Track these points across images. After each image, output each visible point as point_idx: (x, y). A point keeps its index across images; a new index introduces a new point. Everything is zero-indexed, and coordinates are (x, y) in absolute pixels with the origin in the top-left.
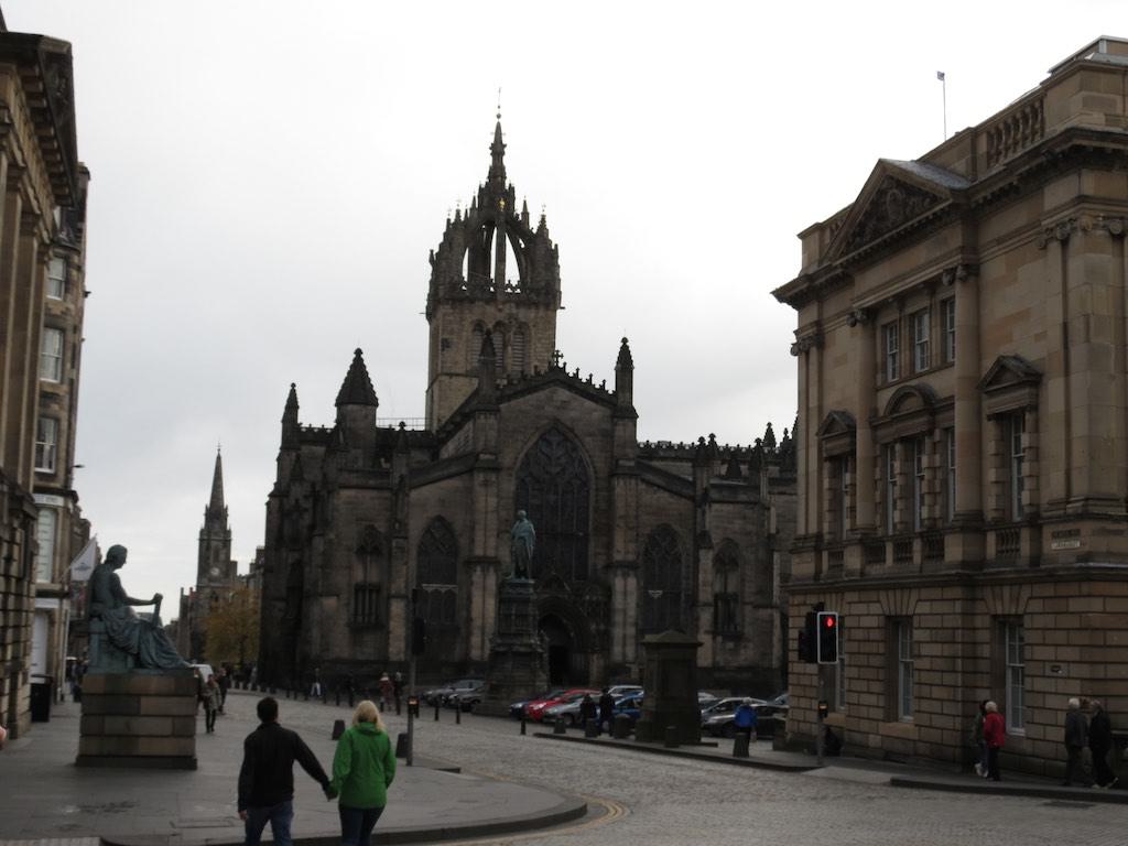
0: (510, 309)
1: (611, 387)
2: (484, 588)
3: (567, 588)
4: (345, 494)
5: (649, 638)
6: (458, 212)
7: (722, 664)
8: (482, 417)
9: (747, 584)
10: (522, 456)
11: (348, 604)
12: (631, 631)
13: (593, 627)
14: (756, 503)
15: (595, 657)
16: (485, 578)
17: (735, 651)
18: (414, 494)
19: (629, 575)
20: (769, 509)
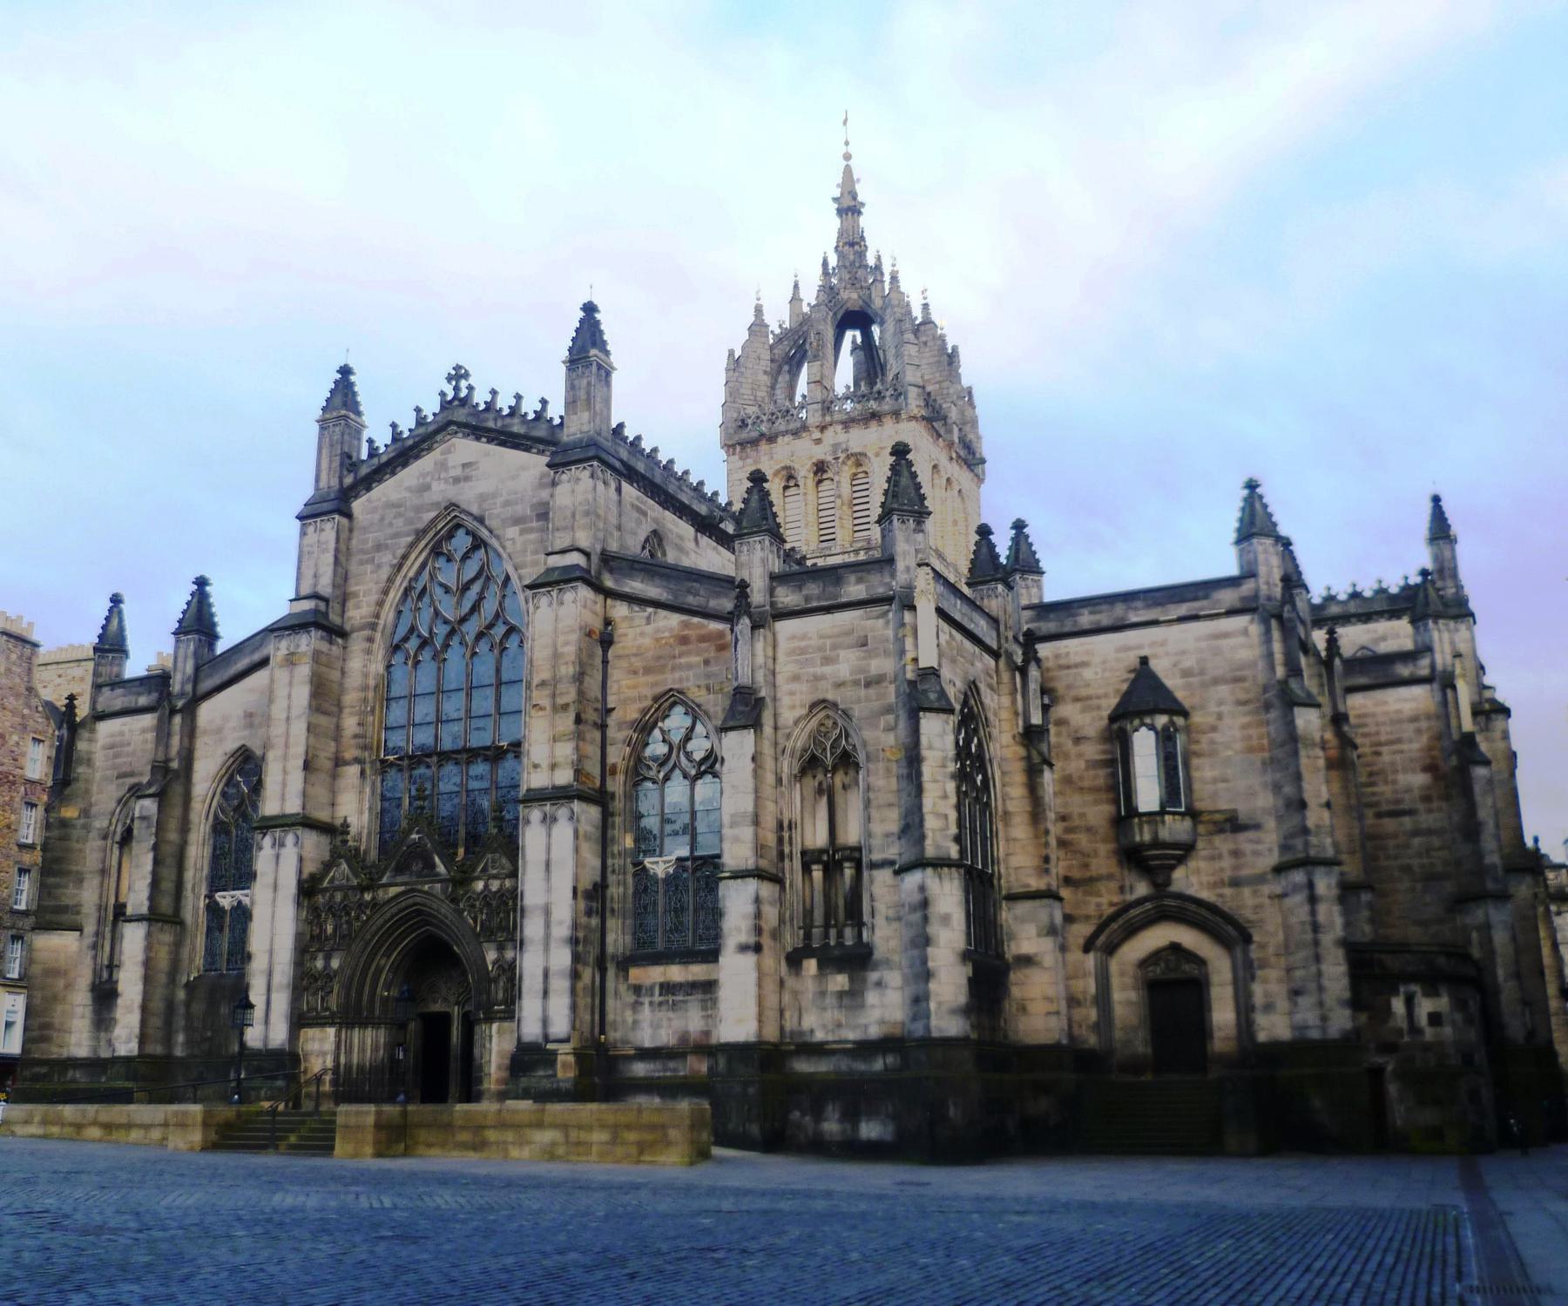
0: (835, 435)
1: (555, 411)
2: (275, 888)
3: (441, 868)
4: (105, 728)
5: (637, 974)
6: (759, 311)
7: (819, 1036)
8: (311, 529)
9: (874, 813)
10: (395, 595)
11: (94, 946)
12: (562, 958)
13: (491, 956)
14: (887, 600)
15: (495, 1026)
16: (278, 857)
17: (852, 998)
18: (207, 712)
19: (554, 820)
20: (913, 608)
